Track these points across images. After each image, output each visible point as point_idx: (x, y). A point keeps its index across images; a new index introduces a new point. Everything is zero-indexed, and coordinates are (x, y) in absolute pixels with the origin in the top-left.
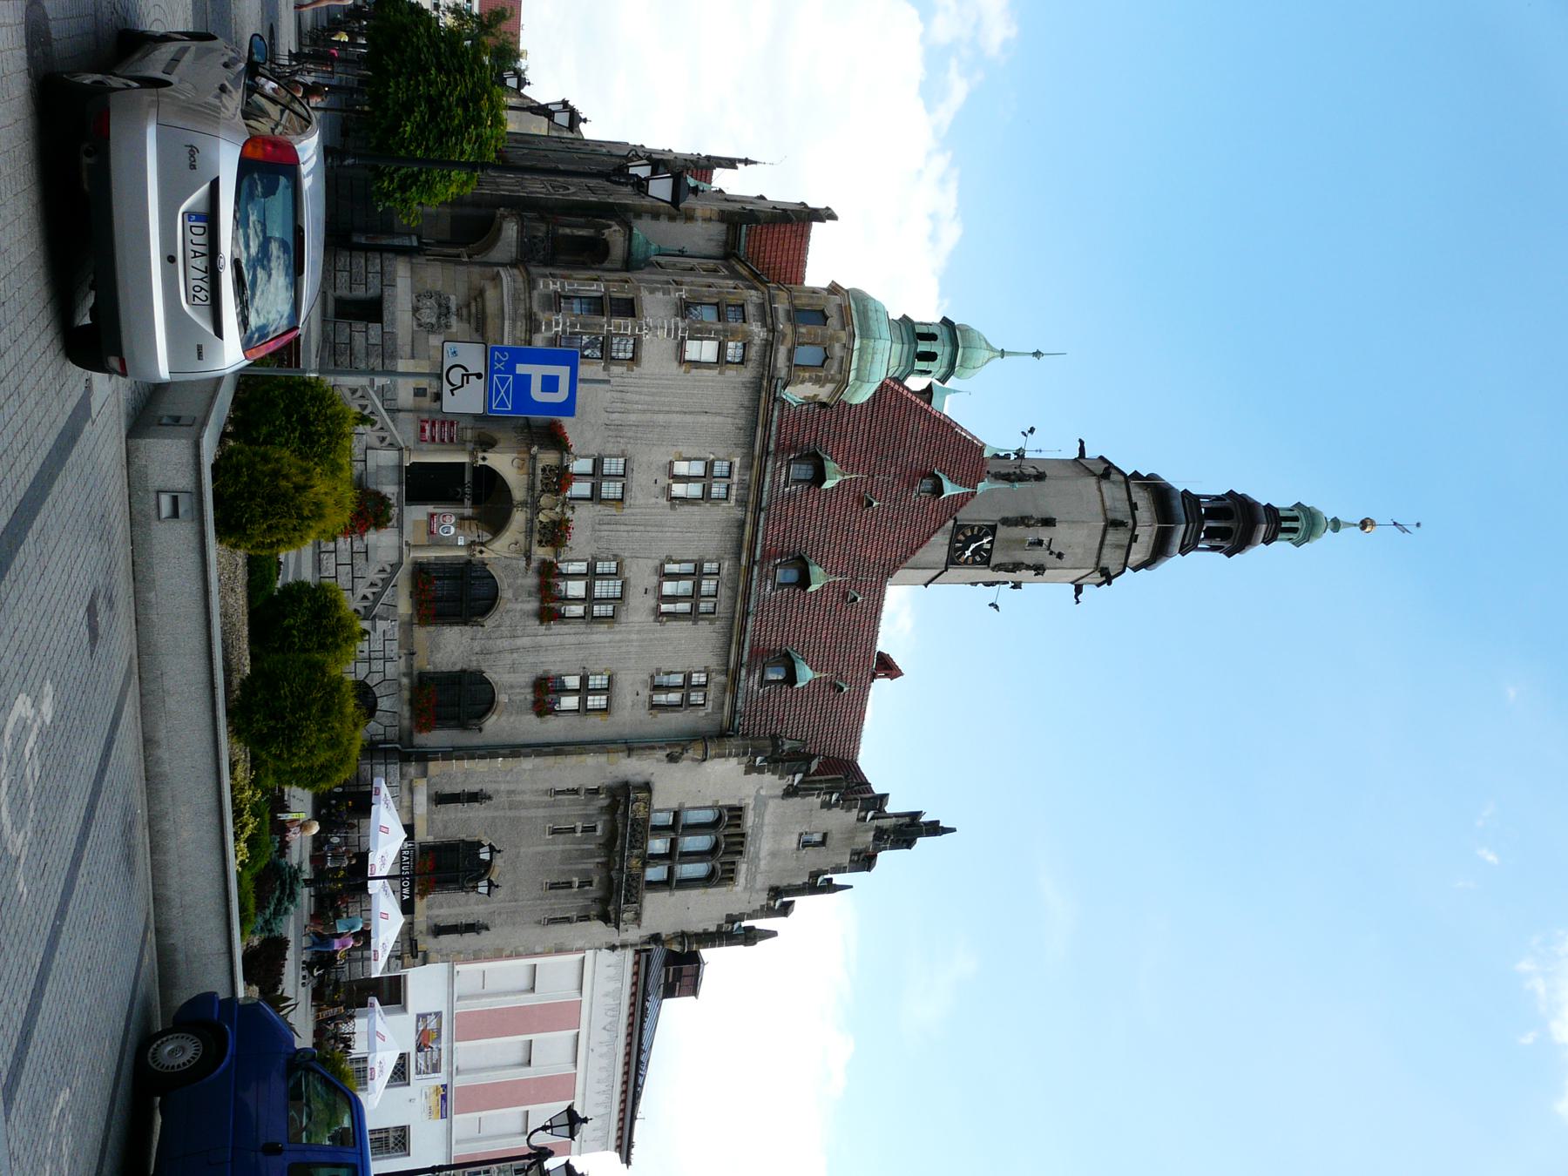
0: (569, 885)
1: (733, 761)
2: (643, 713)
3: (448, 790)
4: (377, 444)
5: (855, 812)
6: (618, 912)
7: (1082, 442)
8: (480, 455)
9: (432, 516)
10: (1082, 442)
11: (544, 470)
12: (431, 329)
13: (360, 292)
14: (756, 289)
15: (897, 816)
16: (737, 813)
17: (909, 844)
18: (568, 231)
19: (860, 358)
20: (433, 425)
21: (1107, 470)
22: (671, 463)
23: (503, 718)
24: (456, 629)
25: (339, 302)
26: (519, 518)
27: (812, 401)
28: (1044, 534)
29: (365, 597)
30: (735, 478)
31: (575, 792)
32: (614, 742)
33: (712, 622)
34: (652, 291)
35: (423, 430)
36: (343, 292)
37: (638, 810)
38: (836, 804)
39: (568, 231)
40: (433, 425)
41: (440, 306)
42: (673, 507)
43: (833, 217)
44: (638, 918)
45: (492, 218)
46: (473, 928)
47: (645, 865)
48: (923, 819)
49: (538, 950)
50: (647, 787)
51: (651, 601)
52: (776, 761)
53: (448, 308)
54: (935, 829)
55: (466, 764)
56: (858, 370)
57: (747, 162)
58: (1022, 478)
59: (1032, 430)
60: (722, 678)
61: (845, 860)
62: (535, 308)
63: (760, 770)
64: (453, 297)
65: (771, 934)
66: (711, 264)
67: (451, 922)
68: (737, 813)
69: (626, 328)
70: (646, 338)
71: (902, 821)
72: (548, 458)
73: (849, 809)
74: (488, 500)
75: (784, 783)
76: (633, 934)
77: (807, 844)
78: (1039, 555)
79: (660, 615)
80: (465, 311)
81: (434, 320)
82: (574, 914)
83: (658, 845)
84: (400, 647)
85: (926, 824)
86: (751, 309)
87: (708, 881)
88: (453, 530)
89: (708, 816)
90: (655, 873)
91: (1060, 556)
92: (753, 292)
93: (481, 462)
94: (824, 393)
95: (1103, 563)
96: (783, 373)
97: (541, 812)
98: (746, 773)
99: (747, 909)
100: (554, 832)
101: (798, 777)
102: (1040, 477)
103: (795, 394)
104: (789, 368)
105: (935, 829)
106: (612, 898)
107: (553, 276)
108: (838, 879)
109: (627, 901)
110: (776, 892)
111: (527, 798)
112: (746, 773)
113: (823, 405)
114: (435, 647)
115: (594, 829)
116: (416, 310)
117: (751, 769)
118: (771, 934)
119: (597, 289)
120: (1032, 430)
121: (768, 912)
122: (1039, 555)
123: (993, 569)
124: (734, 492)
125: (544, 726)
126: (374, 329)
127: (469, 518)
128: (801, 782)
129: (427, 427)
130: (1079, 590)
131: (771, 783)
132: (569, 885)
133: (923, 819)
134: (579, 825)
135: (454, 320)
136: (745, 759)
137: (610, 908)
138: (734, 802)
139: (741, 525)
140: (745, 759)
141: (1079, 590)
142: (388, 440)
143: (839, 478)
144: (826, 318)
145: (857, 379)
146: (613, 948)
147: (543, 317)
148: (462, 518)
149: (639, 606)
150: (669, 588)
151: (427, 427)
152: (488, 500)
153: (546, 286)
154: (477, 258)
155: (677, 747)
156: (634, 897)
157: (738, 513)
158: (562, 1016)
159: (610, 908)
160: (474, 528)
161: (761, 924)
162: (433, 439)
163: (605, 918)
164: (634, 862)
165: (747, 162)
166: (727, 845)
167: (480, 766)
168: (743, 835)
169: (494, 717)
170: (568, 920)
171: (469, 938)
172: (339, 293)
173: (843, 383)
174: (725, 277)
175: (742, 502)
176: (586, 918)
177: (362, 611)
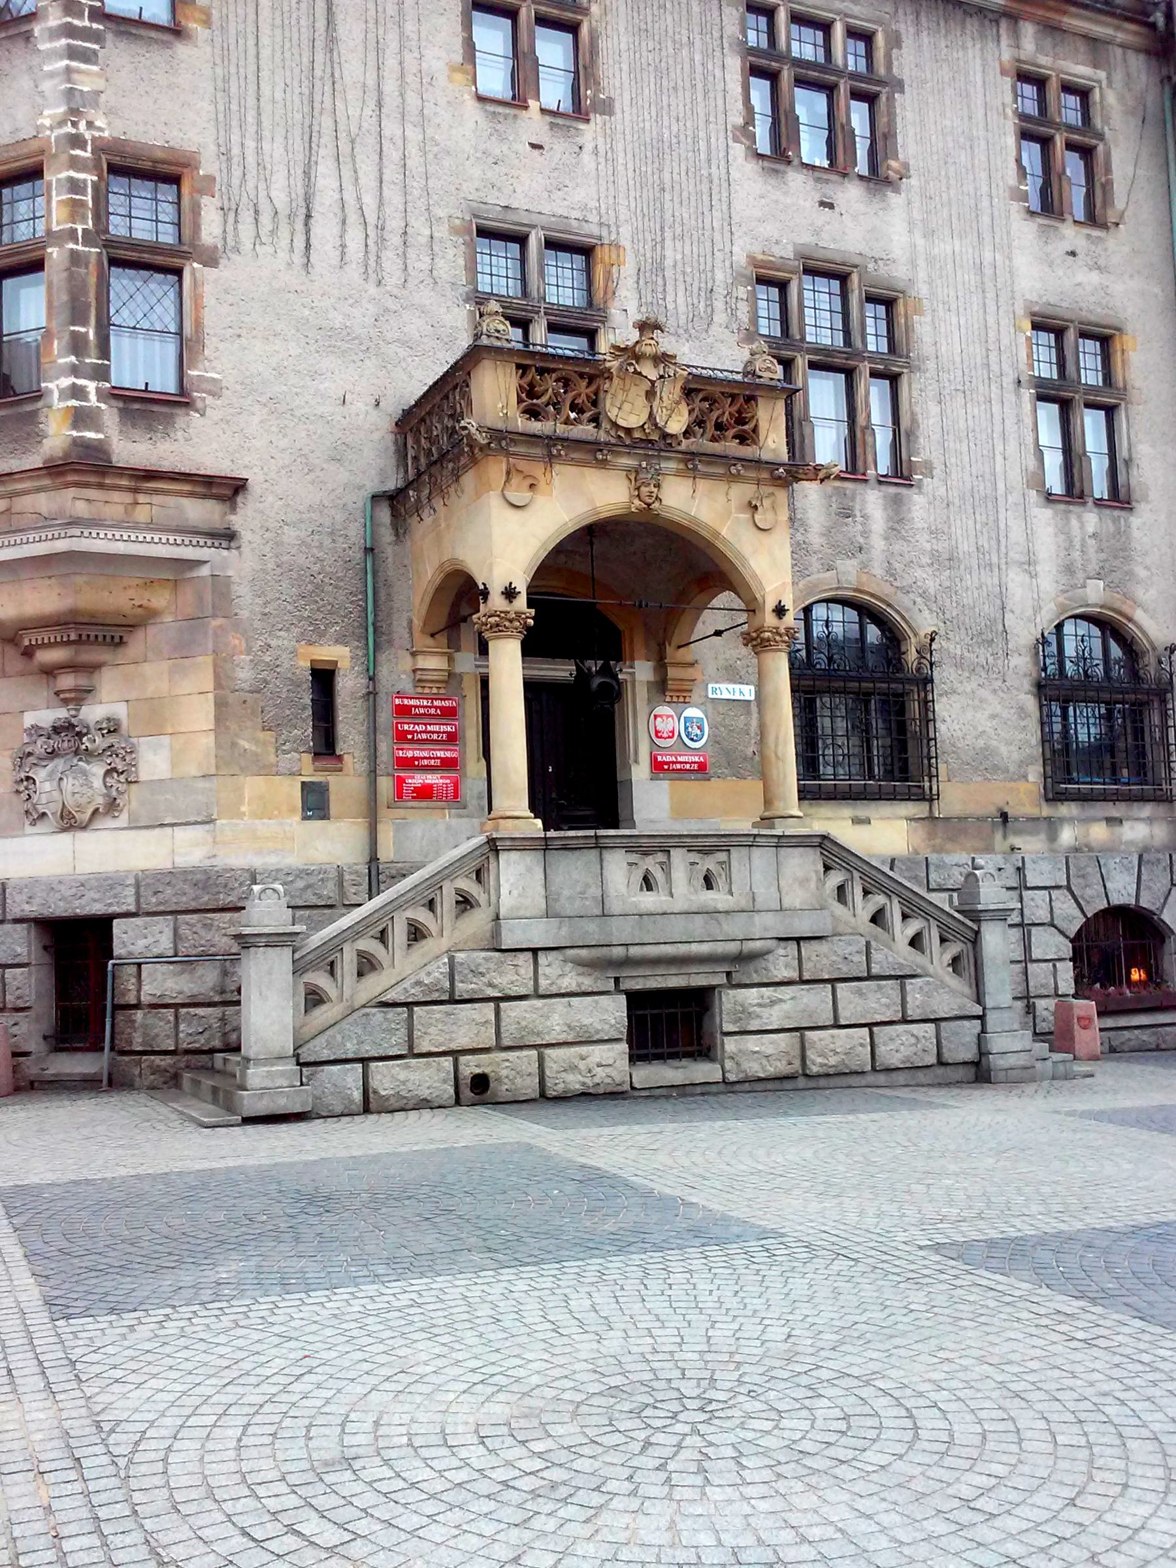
2: (1117, 245)
4: (477, 922)
8: (497, 602)
9: (658, 767)
11: (533, 413)
12: (122, 771)
20: (407, 764)
22: (481, 99)
23: (1140, 593)
24: (942, 707)
26: (687, 500)
29: (915, 942)
33: (895, 41)
35: (424, 793)
40: (407, 764)
41: (53, 754)
42: (606, 108)
51: (851, 194)
53: (57, 730)
60: (1028, 30)
62: (34, 461)
64: (29, 719)
69: (75, 186)
70: (104, 126)
74: (611, 609)
79: (879, 178)
80: (67, 681)
81: (97, 770)
84: (989, 849)
88: (692, 712)
114: (985, 763)
116: (69, 822)
125: (1153, 495)
126: (128, 938)
127: (661, 665)
129: (418, 779)
135: (92, 713)
142: (467, 884)
147: (57, 435)
148: (661, 687)
149: (858, 226)
150: (811, 147)
151: (418, 779)
160: (684, 655)
162: (449, 764)
169: (1139, 615)
177: (954, 949)
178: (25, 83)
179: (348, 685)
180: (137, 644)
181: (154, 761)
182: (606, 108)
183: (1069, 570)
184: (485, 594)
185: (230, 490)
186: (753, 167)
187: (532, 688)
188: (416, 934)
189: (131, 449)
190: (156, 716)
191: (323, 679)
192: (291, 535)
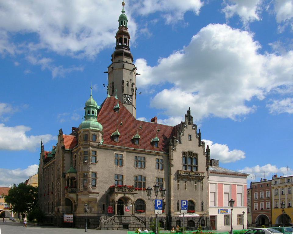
0: (196, 186)
1: (174, 154)
2: (163, 171)
3: (177, 208)
5: (185, 129)
7: (104, 72)
10: (104, 72)
14: (80, 148)
15: (186, 120)
16: (184, 153)
17: (192, 117)
18: (70, 185)
19: (94, 127)
21: (111, 67)
26: (127, 195)
27: (103, 137)
28: (125, 83)
31: (178, 185)
37: (182, 173)
38: (183, 133)
39: (70, 185)
43: (61, 130)
44: (203, 173)
45: (66, 198)
46: (202, 204)
47: (193, 171)
48: (187, 114)
49: (207, 191)
52: (174, 145)
54: (189, 112)
55: (172, 205)
56: (96, 128)
58: (113, 87)
59: (104, 85)
63: (176, 148)
65: (208, 146)
67: (201, 207)
68: (184, 153)
71: (187, 119)
72: (116, 190)
75: (178, 143)
76: (206, 174)
77: (191, 139)
78: (130, 84)
83: (189, 170)
85: (188, 114)
87: (197, 159)
89: (184, 158)
90: (194, 170)
91: (131, 80)
93: (117, 202)
94: (101, 135)
95: (132, 69)
96: (97, 143)
98: (176, 151)
99: (203, 151)
101: (177, 141)
102: (113, 83)
103: (101, 141)
104: (97, 142)
105: (189, 112)
106: (199, 178)
107: (80, 187)
108: (198, 132)
109: (200, 175)
110: (200, 145)
111: (179, 194)
112: (176, 151)
113: (103, 134)
117: (175, 150)
118: (208, 146)
119: (82, 180)
120: (104, 85)
121: (204, 147)
122: (130, 84)
123: (133, 95)
128: (178, 140)
130: (137, 74)
132: (196, 186)
133: (187, 114)
134: (184, 184)
136: (173, 151)
137: (201, 178)
138: (182, 153)
139: (127, 152)
140: (173, 151)
141: (137, 74)
142: (114, 218)
143: (118, 132)
144: (86, 134)
145: (98, 128)
146: (208, 178)
149: (142, 172)
152: (123, 201)
153: (82, 189)
154: (76, 202)
156: (199, 173)
158: (220, 187)
160: (128, 203)
161: (206, 148)
163: (202, 179)
166: (190, 155)
167: (172, 202)
168: (188, 152)
173: (99, 131)
174: (77, 154)
175: (123, 151)
176: (202, 182)
179: (105, 205)
181: (93, 210)
185: (98, 193)
186: (134, 168)
187: (118, 205)
188: (110, 221)
189: (93, 191)
190: (93, 207)
191: (104, 205)
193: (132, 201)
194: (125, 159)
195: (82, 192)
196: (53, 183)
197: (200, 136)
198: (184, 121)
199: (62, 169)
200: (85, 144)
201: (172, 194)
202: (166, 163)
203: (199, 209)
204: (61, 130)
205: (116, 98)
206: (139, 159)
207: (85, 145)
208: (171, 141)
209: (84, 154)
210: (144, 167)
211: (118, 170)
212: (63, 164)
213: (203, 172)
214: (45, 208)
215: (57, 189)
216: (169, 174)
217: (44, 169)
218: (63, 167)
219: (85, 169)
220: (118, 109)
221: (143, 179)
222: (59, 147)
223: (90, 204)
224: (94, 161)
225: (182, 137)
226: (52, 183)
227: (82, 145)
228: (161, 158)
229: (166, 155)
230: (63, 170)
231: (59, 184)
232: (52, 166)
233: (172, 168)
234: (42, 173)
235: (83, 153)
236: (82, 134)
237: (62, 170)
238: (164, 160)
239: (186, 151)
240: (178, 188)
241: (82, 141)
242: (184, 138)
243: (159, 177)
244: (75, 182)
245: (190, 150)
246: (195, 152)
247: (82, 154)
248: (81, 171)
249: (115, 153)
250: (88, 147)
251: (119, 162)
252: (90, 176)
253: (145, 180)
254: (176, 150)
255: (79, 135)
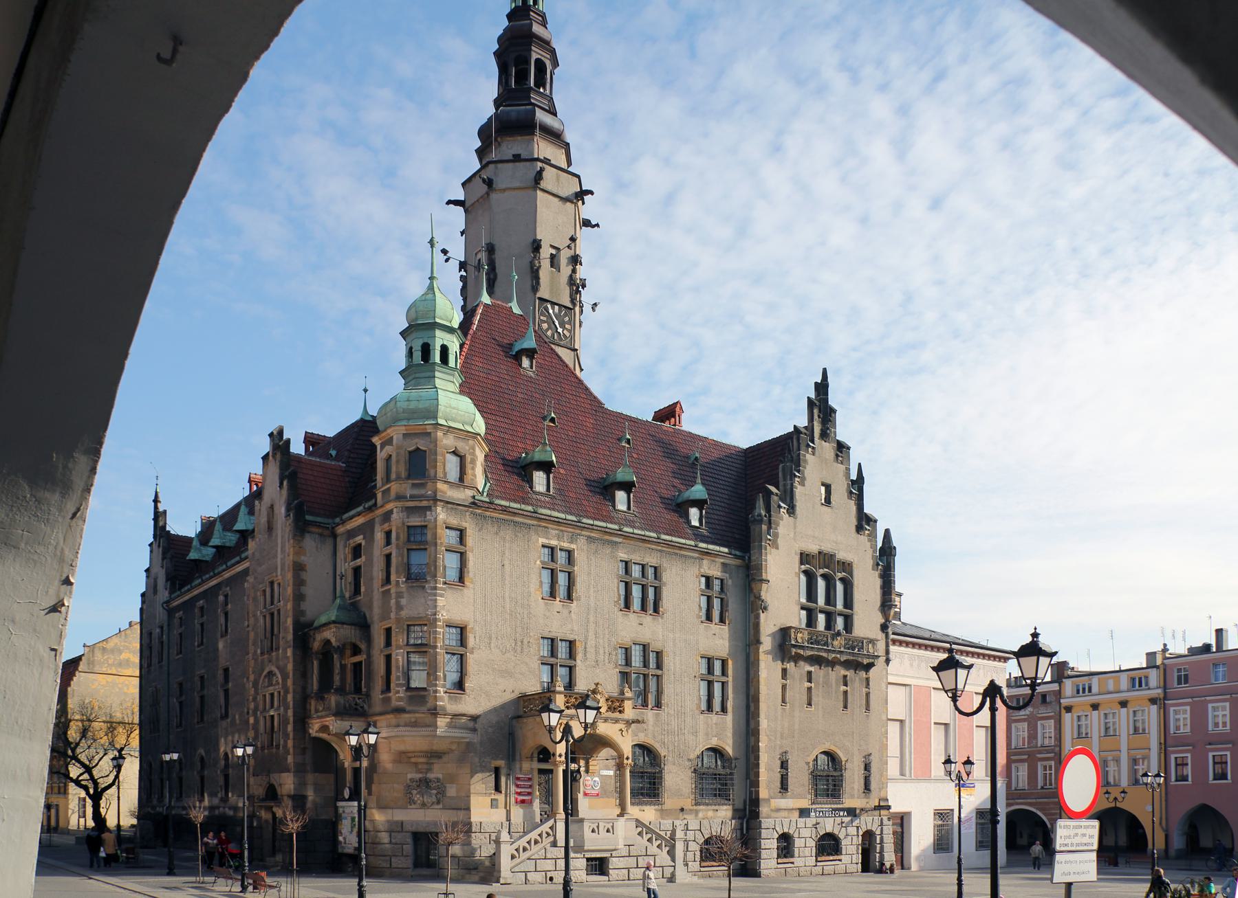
0: (846, 693)
6: (869, 656)
12: (441, 792)
13: (408, 848)
14: (391, 512)
15: (811, 419)
17: (833, 411)
25: (416, 865)
30: (554, 543)
31: (784, 687)
32: (748, 656)
34: (399, 608)
36: (409, 862)
37: (802, 637)
46: (867, 767)
48: (813, 396)
50: (784, 632)
51: (648, 619)
54: (822, 388)
57: (156, 501)
61: (843, 467)
63: (776, 535)
64: (409, 776)
66: (344, 551)
68: (805, 558)
73: (806, 461)
81: (434, 792)
82: (865, 690)
86: (415, 521)
92: (394, 516)
97: (797, 714)
99: (870, 552)
100: (810, 704)
105: (822, 388)
115: (810, 673)
116: (424, 805)
124: (566, 545)
131: (784, 525)
132: (846, 693)
133: (813, 396)
134: (807, 684)
138: (797, 558)
153: (400, 699)
155: (753, 605)
157: (582, 541)
159: (866, 661)
164: (836, 643)
165: (156, 501)
170: (868, 695)
171: (874, 769)
172: (411, 866)
174: (370, 539)
178: (423, 600)
180: (445, 758)
182: (579, 599)
183: (707, 734)
184: (554, 755)
192: (490, 730)
193: (621, 756)
194: (581, 569)
195: (399, 711)
196: (226, 670)
197: (861, 490)
198: (803, 422)
199: (290, 606)
200: (416, 492)
201: (764, 723)
202: (740, 594)
203: (856, 787)
204: (281, 432)
205: (516, 310)
206: (636, 571)
207: (413, 497)
208: (760, 503)
209: (409, 540)
210: (656, 610)
211: (559, 620)
212: (299, 583)
213: (872, 636)
214: (181, 779)
215: (260, 698)
216: (748, 641)
217: (171, 612)
218: (299, 597)
219: (412, 607)
220: (531, 353)
221: (652, 657)
222: (272, 507)
223: (436, 767)
224: (452, 574)
225: (799, 491)
226: (221, 672)
227: (399, 498)
228: (716, 572)
229: (738, 562)
230: (298, 613)
231: (270, 674)
232: (221, 598)
233: (762, 616)
234: (158, 630)
235: (403, 537)
236: (399, 447)
237: (291, 614)
238: (730, 582)
239: (813, 548)
240: (784, 701)
241: (398, 478)
242: (807, 492)
243: (711, 654)
244: (357, 666)
245: (827, 547)
246: (841, 555)
247: (398, 539)
248: (393, 615)
249: (542, 541)
250: (429, 508)
251: (561, 583)
252: (445, 638)
253: (659, 666)
254: (780, 541)
255: (381, 455)
